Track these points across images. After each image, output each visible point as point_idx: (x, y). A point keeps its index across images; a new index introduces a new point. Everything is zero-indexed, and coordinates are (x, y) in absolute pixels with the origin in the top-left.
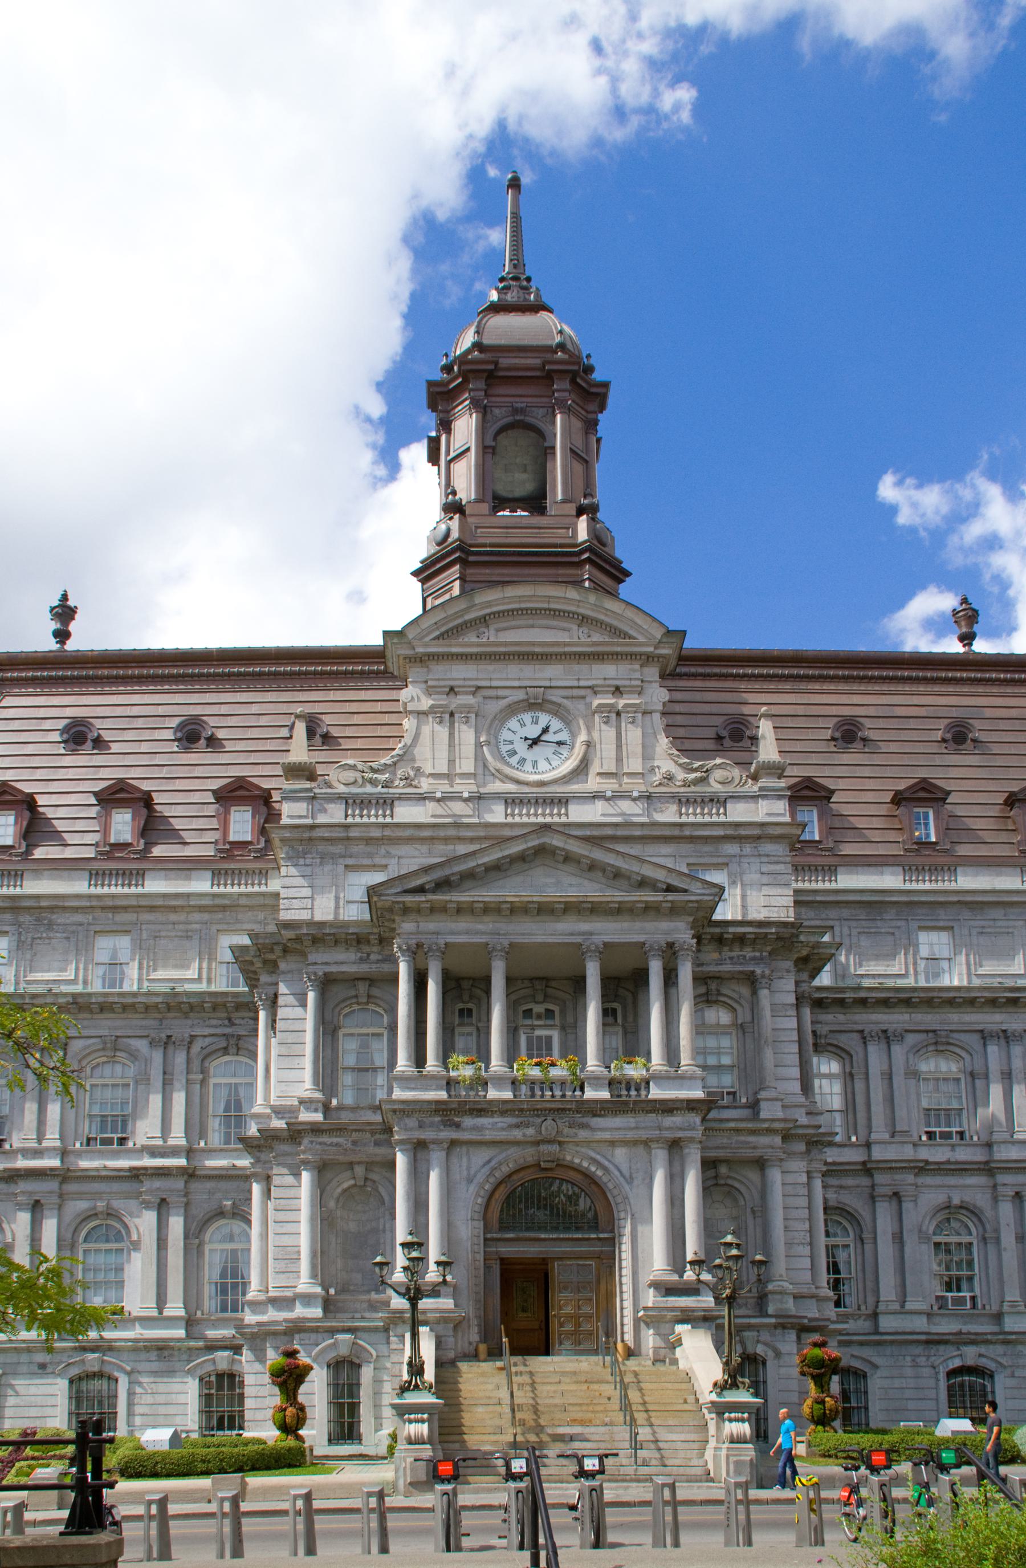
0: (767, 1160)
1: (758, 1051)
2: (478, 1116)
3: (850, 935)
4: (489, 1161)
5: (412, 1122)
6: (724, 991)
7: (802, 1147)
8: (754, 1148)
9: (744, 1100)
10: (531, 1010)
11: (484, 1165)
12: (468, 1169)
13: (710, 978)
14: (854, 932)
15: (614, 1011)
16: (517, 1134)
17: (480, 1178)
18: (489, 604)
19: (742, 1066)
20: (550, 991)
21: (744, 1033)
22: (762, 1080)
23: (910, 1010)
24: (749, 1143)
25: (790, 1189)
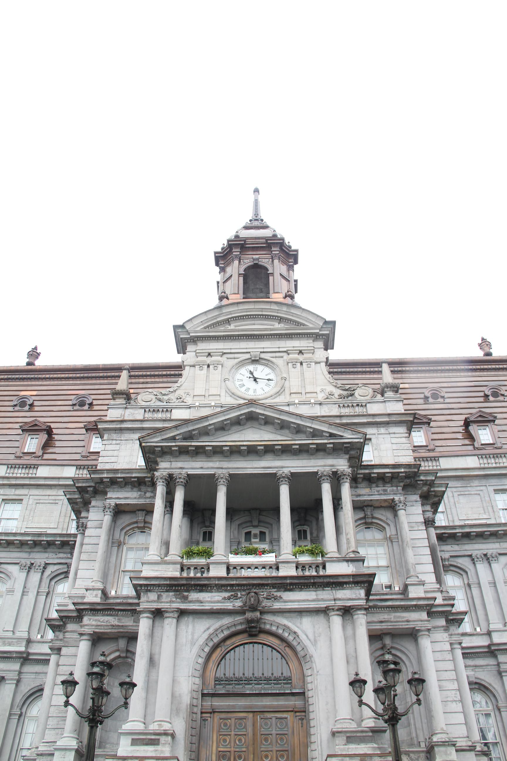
0: (418, 631)
1: (403, 552)
2: (201, 591)
3: (453, 496)
4: (208, 629)
5: (153, 596)
6: (376, 515)
7: (442, 622)
9: (397, 589)
10: (250, 532)
11: (205, 631)
12: (193, 634)
13: (366, 506)
14: (456, 494)
15: (305, 532)
16: (229, 606)
17: (201, 641)
18: (231, 313)
19: (393, 565)
20: (262, 518)
21: (392, 542)
22: (408, 571)
23: (499, 540)
24: (403, 617)
25: (439, 656)
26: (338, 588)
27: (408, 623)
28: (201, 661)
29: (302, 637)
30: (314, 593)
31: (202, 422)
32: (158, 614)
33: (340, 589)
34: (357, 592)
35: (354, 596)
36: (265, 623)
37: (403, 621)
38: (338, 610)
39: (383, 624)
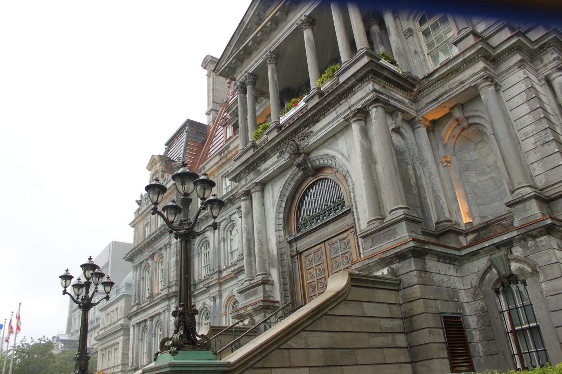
0: (476, 87)
8: (462, 83)
16: (282, 162)
26: (350, 95)
27: (463, 85)
28: (281, 216)
29: (339, 156)
30: (334, 113)
31: (242, 28)
32: (248, 194)
33: (352, 95)
34: (367, 88)
35: (365, 94)
36: (314, 161)
37: (457, 86)
38: (353, 117)
39: (440, 100)
